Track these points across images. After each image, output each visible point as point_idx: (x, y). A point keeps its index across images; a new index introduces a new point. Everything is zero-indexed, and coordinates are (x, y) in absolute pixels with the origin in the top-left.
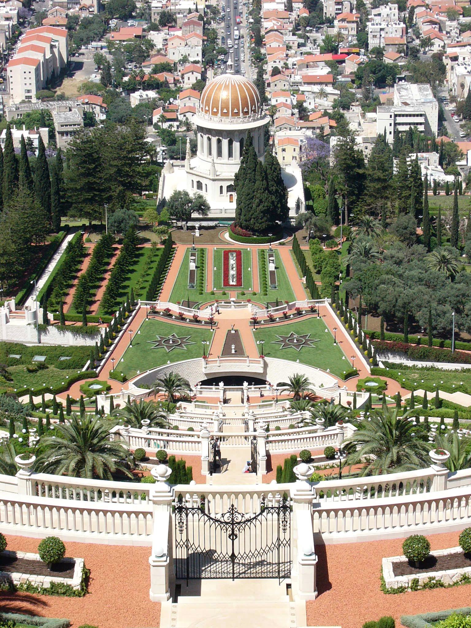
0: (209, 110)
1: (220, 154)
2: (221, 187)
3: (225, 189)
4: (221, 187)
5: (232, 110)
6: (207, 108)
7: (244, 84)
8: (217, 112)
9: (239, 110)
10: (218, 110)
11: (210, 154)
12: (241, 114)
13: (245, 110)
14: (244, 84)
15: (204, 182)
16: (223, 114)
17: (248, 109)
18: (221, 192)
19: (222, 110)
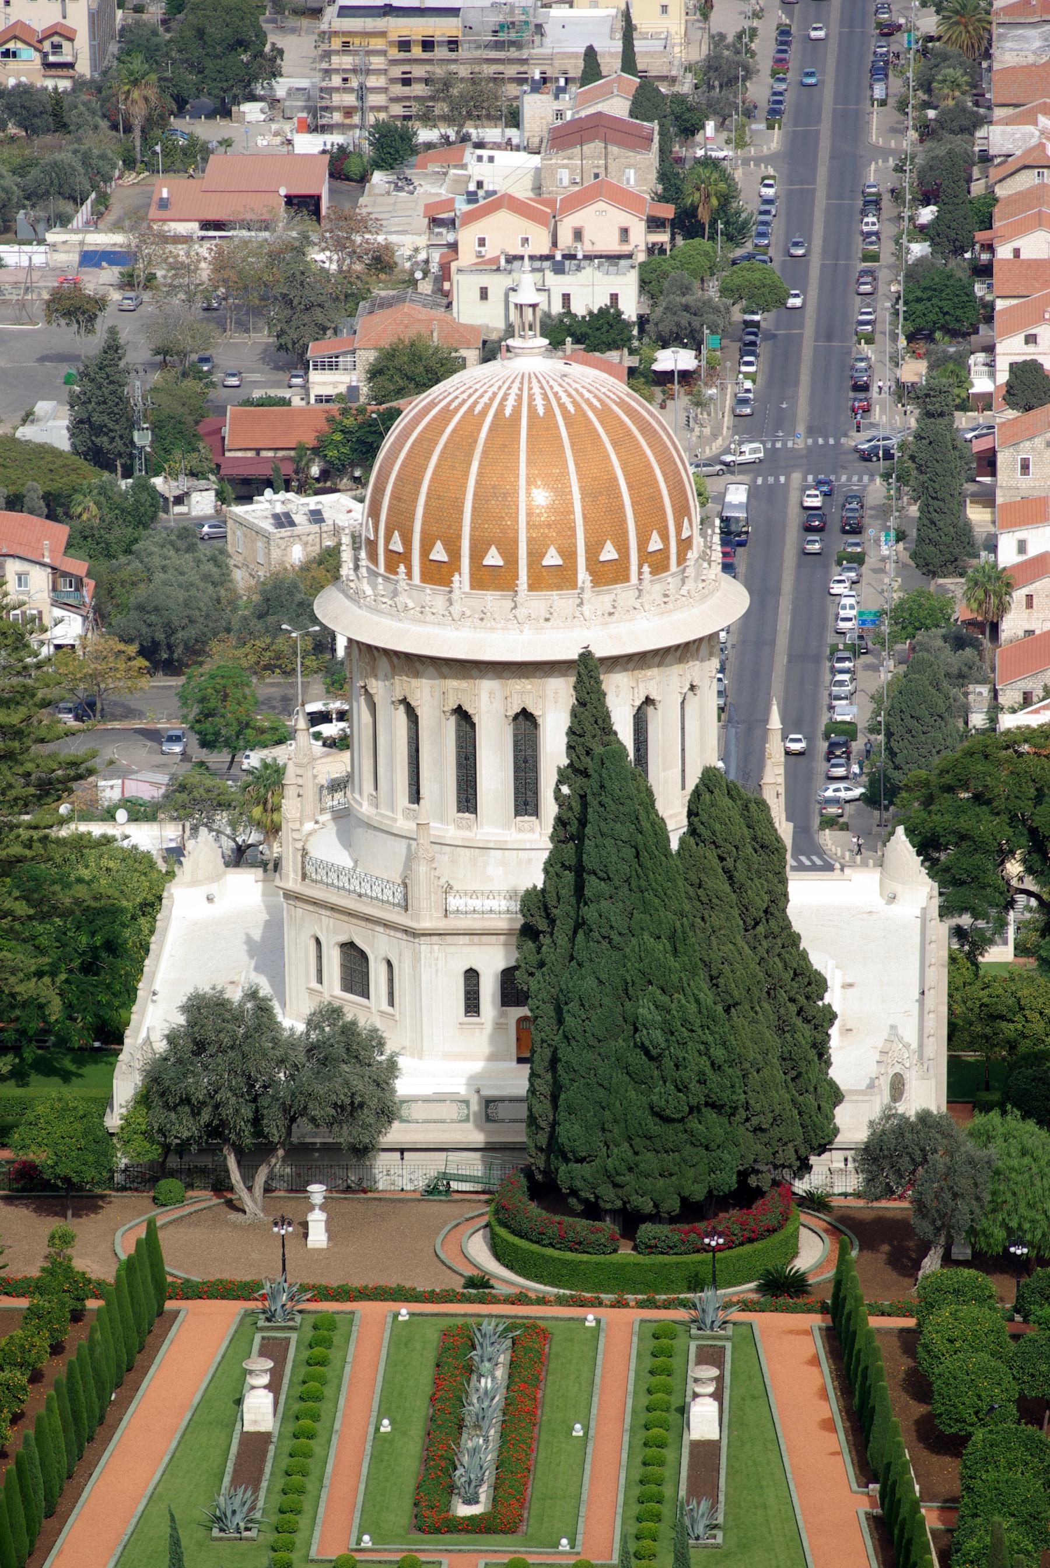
0: (405, 557)
1: (467, 798)
2: (472, 976)
3: (489, 989)
4: (472, 976)
5: (535, 556)
6: (397, 546)
7: (605, 414)
8: (453, 564)
9: (569, 555)
10: (454, 553)
11: (416, 796)
12: (583, 576)
13: (609, 553)
14: (605, 414)
15: (378, 947)
16: (486, 579)
17: (623, 548)
18: (472, 1005)
19: (477, 555)
